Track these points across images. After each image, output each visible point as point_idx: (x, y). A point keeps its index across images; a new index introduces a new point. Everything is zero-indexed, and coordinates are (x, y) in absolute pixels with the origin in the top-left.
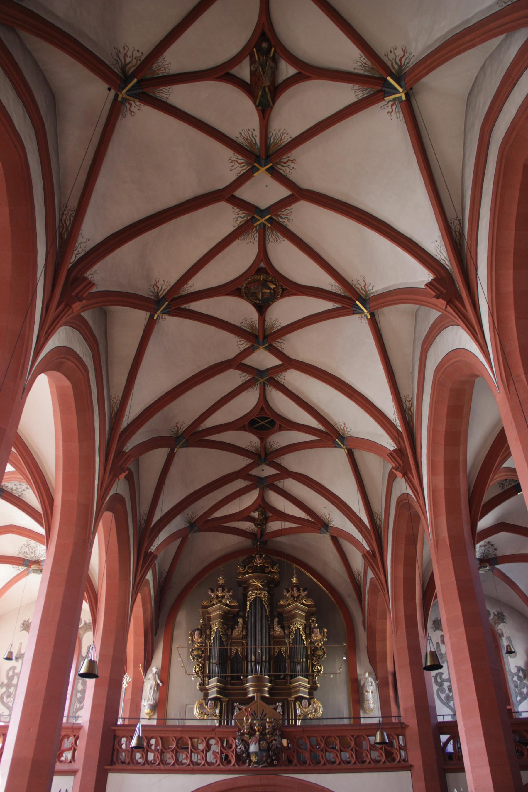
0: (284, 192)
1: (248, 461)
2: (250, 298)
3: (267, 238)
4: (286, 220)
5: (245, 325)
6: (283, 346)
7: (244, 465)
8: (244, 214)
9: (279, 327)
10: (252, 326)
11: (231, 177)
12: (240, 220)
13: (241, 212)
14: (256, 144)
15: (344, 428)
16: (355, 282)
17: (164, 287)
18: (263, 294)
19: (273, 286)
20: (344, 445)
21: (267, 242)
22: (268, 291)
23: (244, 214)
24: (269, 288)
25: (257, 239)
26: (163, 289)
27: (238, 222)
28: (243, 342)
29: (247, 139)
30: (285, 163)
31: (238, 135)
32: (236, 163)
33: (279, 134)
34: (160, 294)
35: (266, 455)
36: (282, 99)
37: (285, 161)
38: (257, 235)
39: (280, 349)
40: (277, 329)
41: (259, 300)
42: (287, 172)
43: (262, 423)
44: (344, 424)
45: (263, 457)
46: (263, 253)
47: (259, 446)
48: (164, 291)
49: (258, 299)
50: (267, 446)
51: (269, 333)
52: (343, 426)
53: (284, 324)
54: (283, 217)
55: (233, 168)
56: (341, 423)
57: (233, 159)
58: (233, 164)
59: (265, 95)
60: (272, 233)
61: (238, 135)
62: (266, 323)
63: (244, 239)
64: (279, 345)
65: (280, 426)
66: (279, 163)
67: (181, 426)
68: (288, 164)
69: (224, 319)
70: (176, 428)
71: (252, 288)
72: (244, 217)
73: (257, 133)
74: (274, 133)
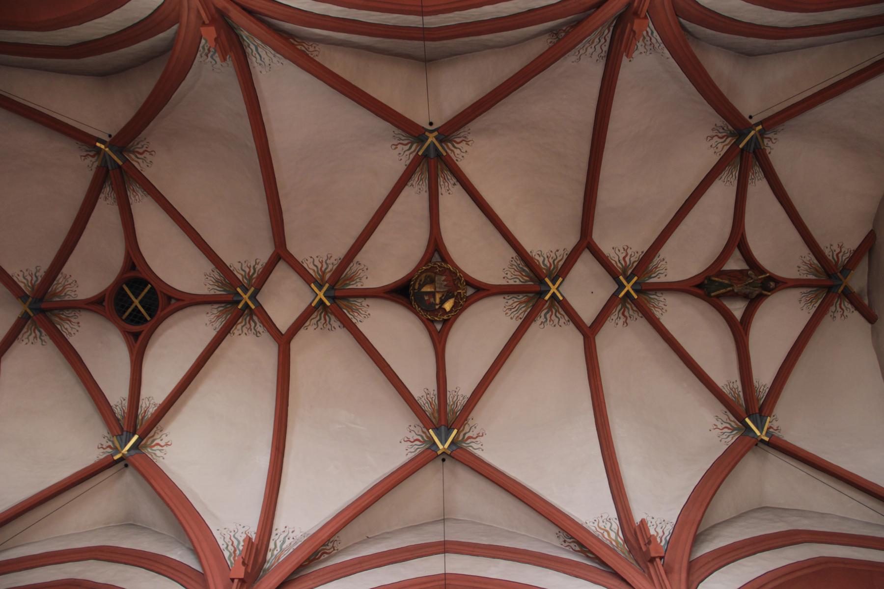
0: (588, 316)
1: (21, 278)
2: (424, 275)
3: (511, 296)
4: (542, 319)
5: (354, 269)
6: (311, 328)
7: (10, 272)
8: (548, 265)
9: (354, 321)
10: (351, 279)
11: (606, 248)
12: (541, 260)
13: (551, 261)
14: (650, 278)
15: (158, 444)
16: (470, 422)
17: (457, 151)
18: (432, 294)
19: (448, 306)
20: (128, 451)
21: (506, 296)
22: (438, 301)
23: (548, 265)
24: (443, 302)
25: (511, 282)
26: (455, 150)
27: (537, 257)
28: (319, 266)
29: (656, 268)
30: (623, 314)
31: (661, 257)
32: (624, 255)
33: (661, 304)
34: (450, 145)
35: (43, 311)
36: (703, 305)
37: (626, 313)
38: (518, 283)
39: (307, 324)
40: (350, 316)
41: (420, 288)
42: (612, 317)
43: (136, 302)
44: (167, 445)
45: (43, 306)
46: (483, 291)
47: (66, 298)
48: (452, 151)
49: (421, 286)
50: (66, 313)
51: (342, 306)
52: (162, 443)
53: (362, 327)
54: (548, 316)
55: (617, 251)
56: (165, 440)
57: (629, 252)
58: (622, 250)
59: (707, 287)
60: (521, 303)
61: (661, 257)
62: (360, 300)
63: (512, 265)
64: (314, 321)
65: (139, 333)
66: (624, 306)
67: (144, 159)
68: (622, 317)
69: (372, 237)
70: (141, 151)
71: (443, 278)
72: (546, 265)
73: (663, 279)
74: (661, 299)
